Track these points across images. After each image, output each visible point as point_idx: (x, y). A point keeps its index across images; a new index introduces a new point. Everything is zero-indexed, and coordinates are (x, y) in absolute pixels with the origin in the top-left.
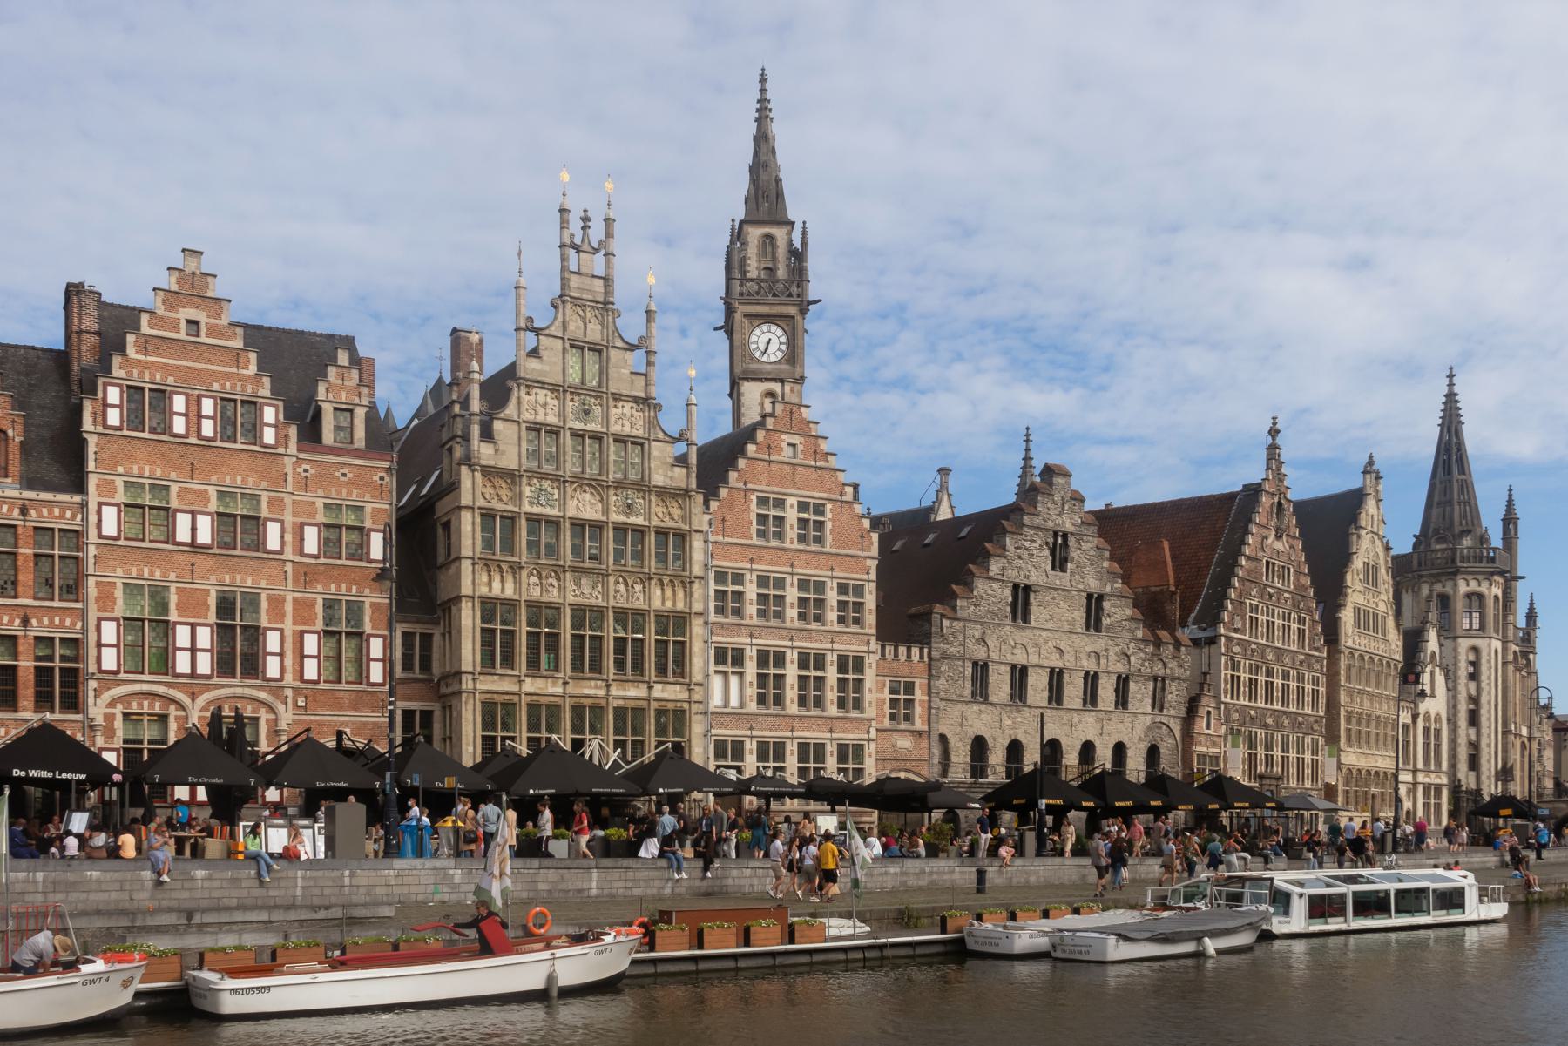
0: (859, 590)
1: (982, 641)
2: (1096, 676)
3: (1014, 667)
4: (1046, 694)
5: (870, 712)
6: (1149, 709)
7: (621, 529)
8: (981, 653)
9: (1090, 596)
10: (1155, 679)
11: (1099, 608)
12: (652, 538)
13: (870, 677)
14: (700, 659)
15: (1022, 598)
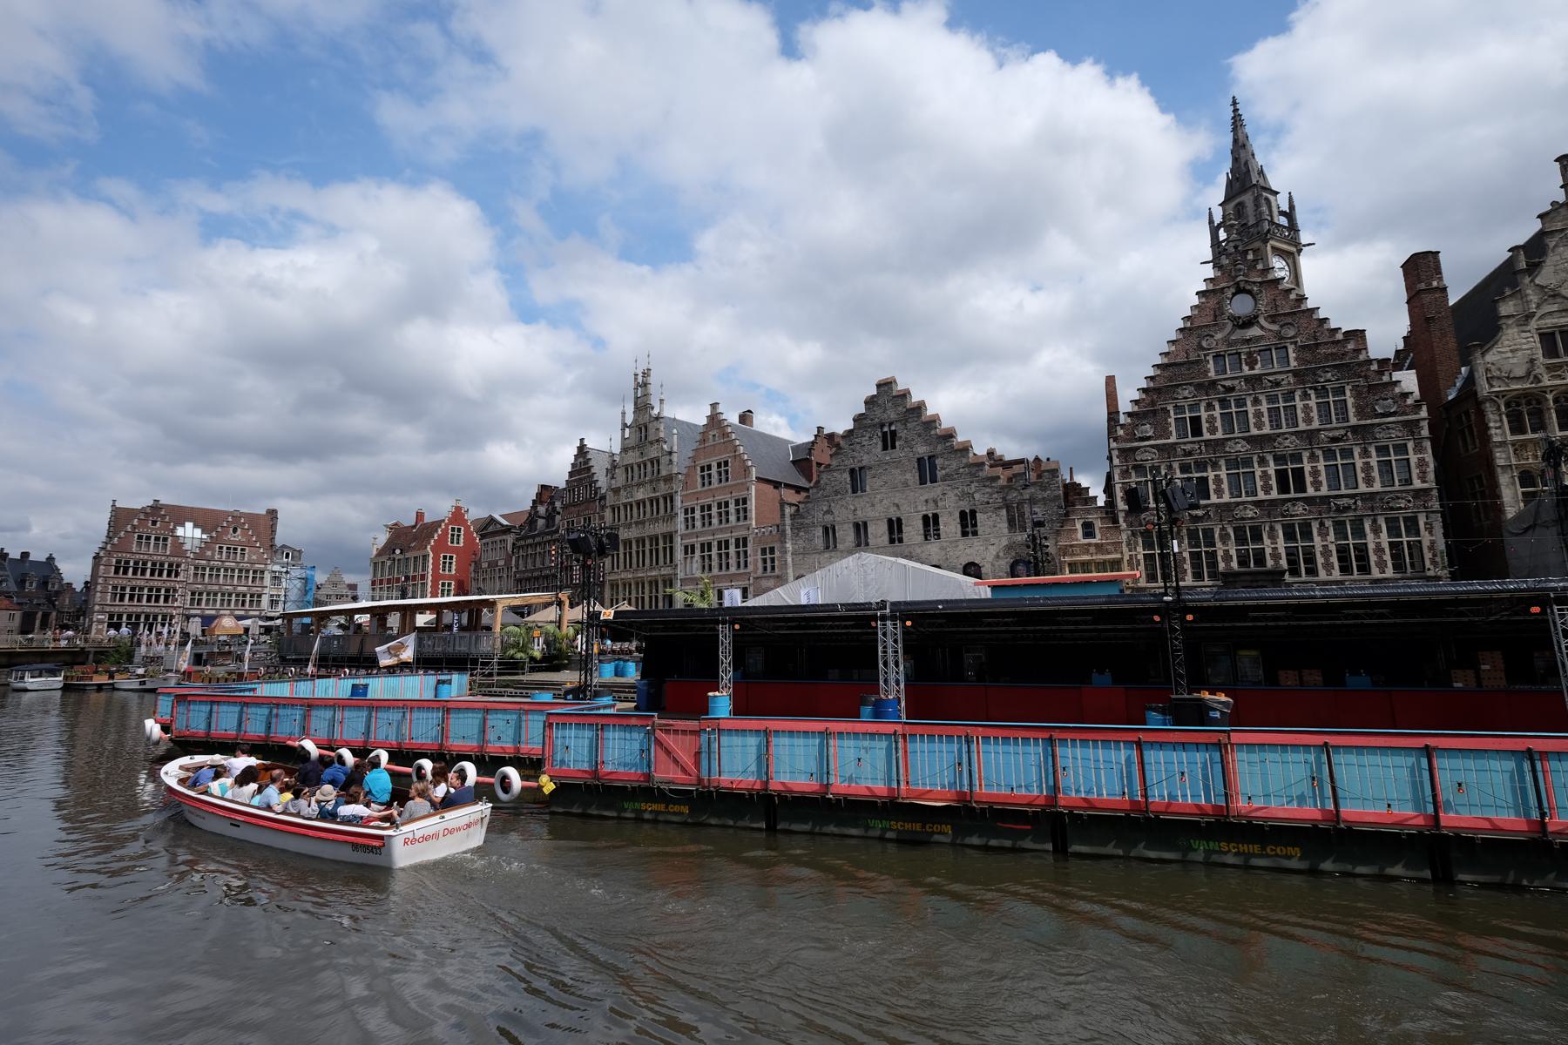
0: (745, 501)
1: (829, 512)
2: (936, 516)
3: (857, 526)
4: (886, 538)
5: (750, 568)
6: (1006, 531)
7: (651, 501)
8: (829, 518)
9: (920, 460)
10: (1008, 507)
11: (933, 468)
12: (661, 501)
13: (749, 549)
14: (679, 554)
15: (857, 479)
